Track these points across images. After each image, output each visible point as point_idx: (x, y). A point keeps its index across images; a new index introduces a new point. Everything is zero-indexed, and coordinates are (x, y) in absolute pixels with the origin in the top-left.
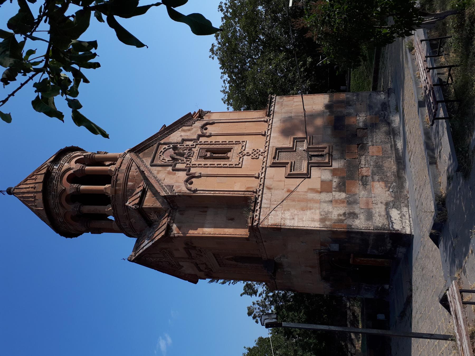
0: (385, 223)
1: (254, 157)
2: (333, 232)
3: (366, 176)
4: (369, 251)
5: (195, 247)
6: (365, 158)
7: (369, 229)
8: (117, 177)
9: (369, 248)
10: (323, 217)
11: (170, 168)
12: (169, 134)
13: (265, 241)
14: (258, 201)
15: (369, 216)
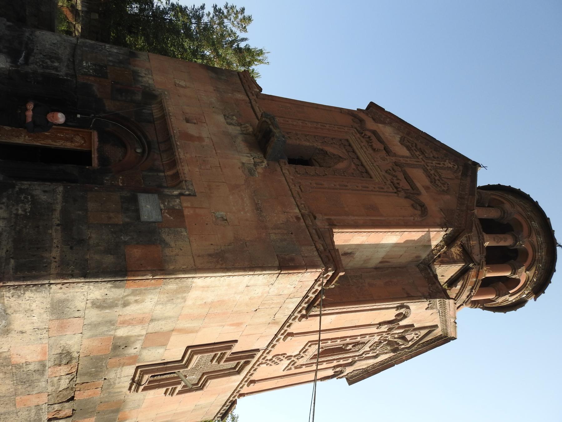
0: (12, 299)
1: (281, 357)
2: (160, 267)
3: (60, 365)
4: (59, 197)
5: (406, 197)
6: (59, 388)
7: (63, 284)
8: (470, 294)
9: (59, 207)
10: (179, 296)
11: (416, 326)
12: (391, 359)
13: (298, 218)
14: (306, 306)
15: (59, 310)
